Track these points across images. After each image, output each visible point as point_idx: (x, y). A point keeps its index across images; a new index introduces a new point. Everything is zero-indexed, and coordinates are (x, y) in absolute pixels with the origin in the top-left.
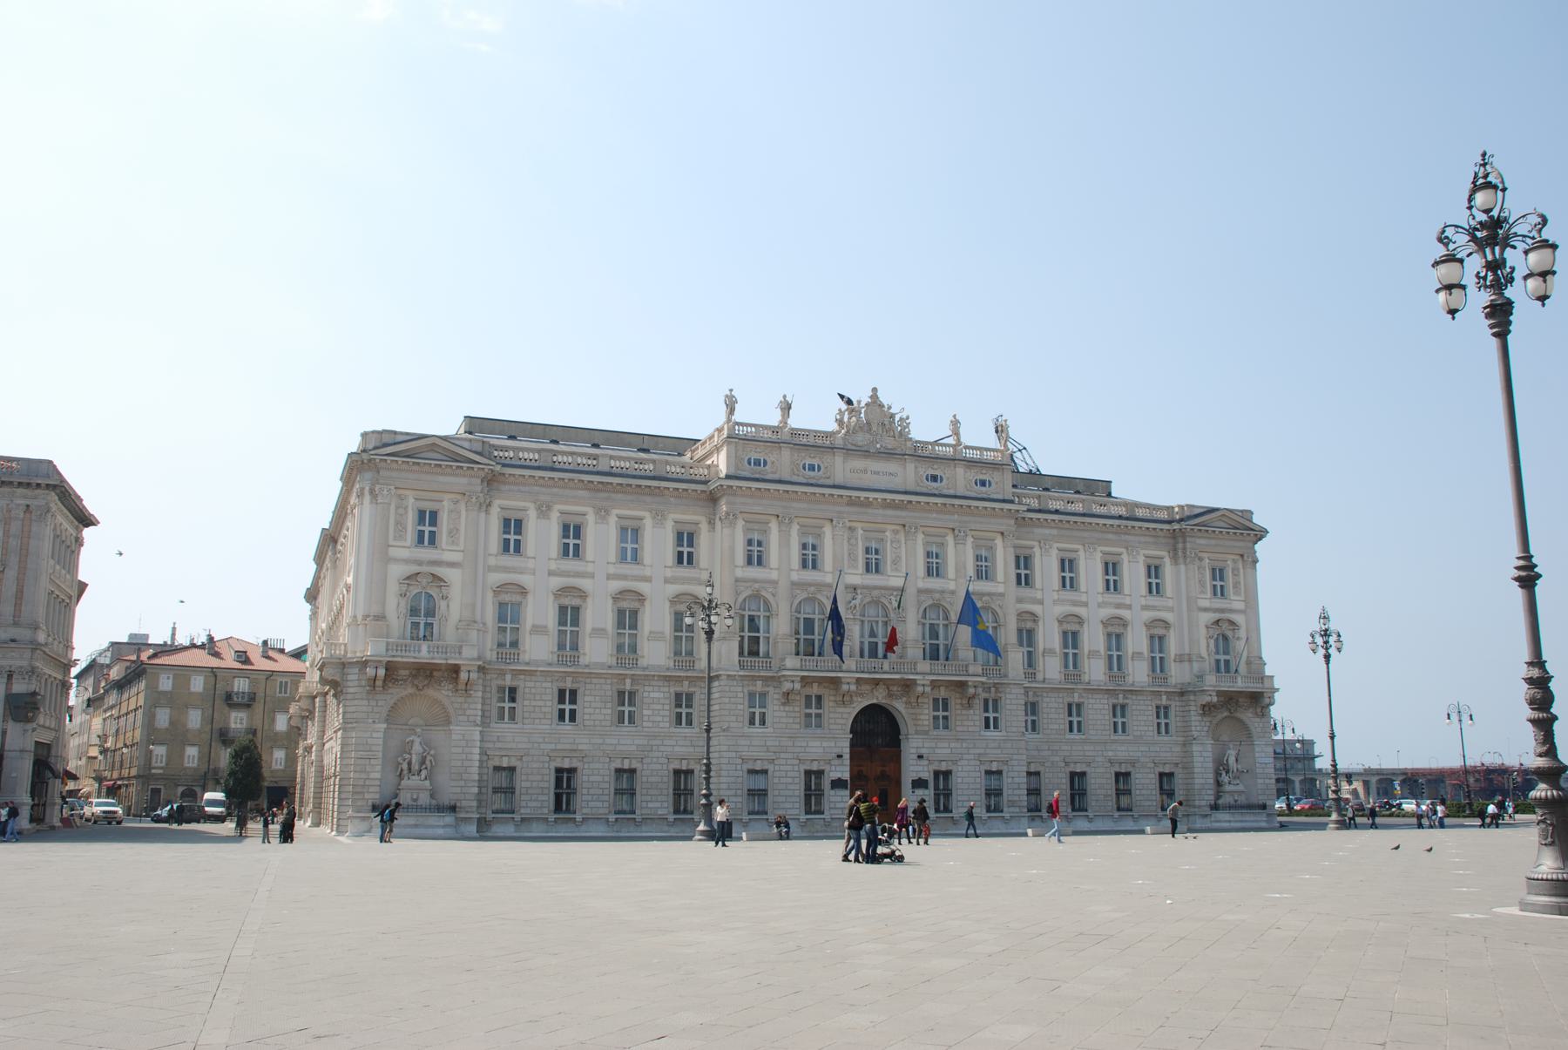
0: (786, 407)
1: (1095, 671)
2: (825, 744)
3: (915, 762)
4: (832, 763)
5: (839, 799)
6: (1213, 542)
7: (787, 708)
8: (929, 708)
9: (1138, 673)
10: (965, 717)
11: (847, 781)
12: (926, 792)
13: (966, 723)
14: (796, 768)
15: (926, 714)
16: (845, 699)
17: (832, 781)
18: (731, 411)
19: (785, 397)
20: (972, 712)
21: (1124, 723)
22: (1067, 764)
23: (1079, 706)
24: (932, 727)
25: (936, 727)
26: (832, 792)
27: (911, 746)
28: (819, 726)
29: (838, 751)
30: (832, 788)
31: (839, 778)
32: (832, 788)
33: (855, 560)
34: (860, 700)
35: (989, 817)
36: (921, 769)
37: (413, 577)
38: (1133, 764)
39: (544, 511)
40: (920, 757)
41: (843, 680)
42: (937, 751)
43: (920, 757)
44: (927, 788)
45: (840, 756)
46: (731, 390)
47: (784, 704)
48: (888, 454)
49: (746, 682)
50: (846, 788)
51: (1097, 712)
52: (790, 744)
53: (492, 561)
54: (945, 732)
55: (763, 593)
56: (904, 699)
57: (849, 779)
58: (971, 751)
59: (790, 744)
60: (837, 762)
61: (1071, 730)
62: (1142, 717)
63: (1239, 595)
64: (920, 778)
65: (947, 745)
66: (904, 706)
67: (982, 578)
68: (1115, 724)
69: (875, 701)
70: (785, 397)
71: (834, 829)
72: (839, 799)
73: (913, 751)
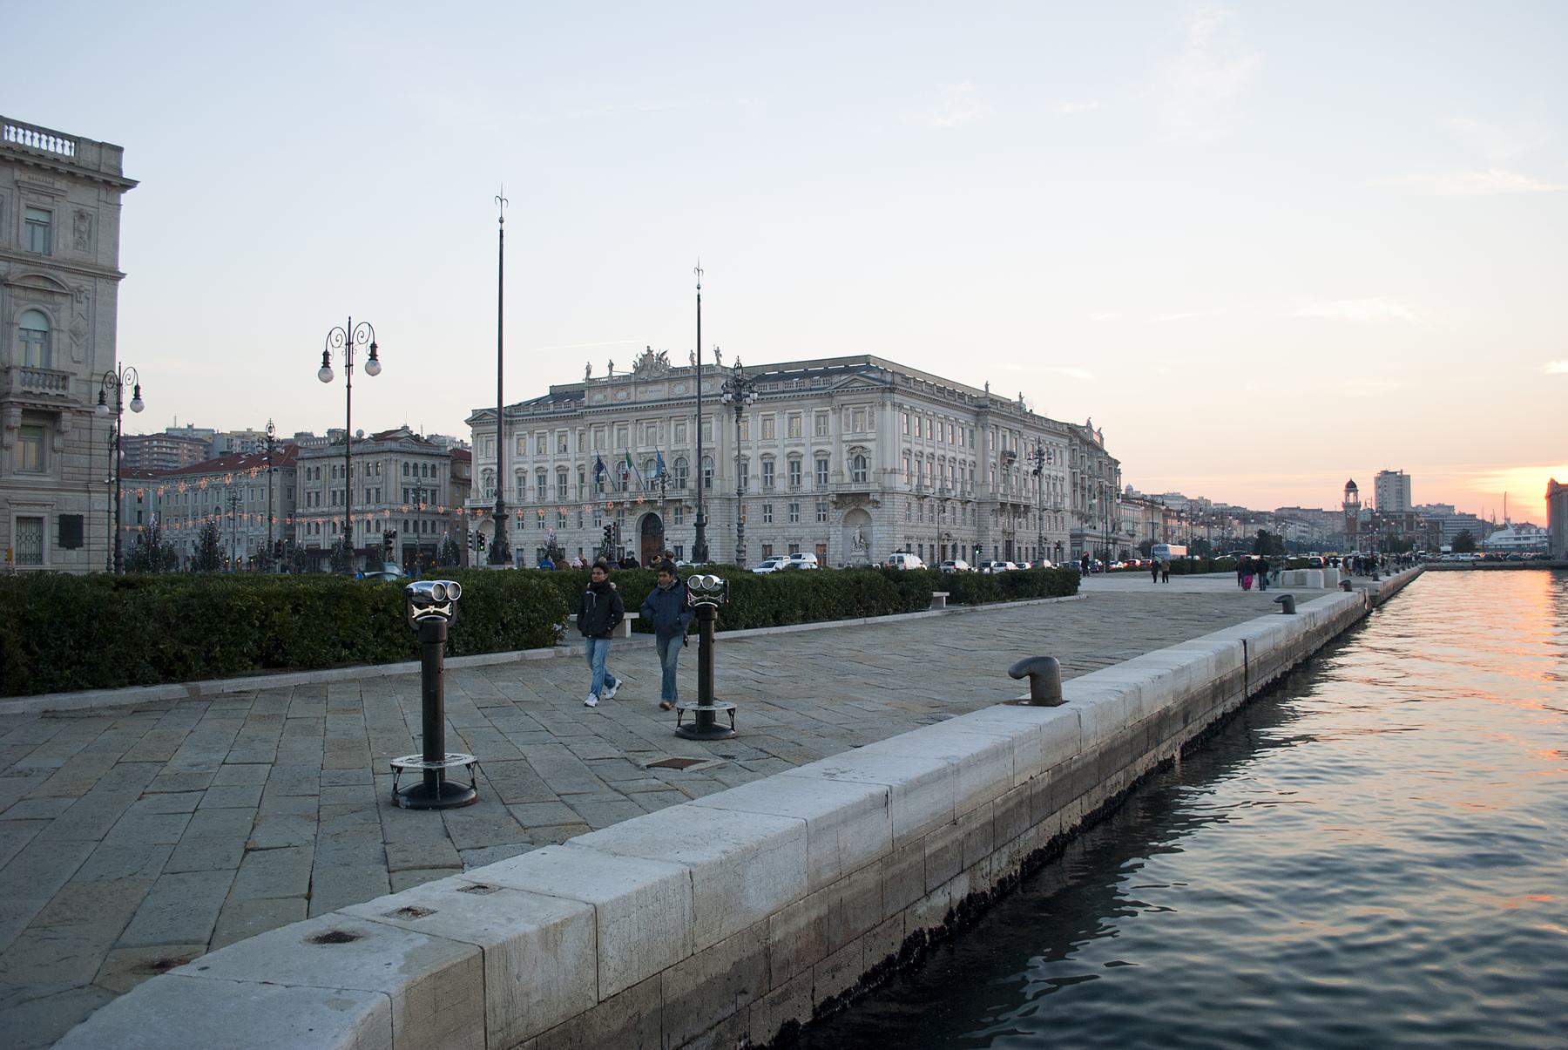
0: (611, 365)
1: (781, 486)
6: (852, 397)
9: (808, 485)
15: (671, 515)
16: (631, 511)
18: (589, 373)
21: (770, 516)
22: (761, 541)
23: (770, 506)
25: (676, 523)
27: (667, 534)
33: (642, 439)
37: (485, 470)
38: (800, 539)
39: (531, 433)
40: (667, 539)
43: (667, 539)
48: (656, 381)
51: (780, 508)
53: (515, 460)
60: (629, 543)
61: (766, 521)
62: (808, 511)
63: (873, 428)
68: (765, 517)
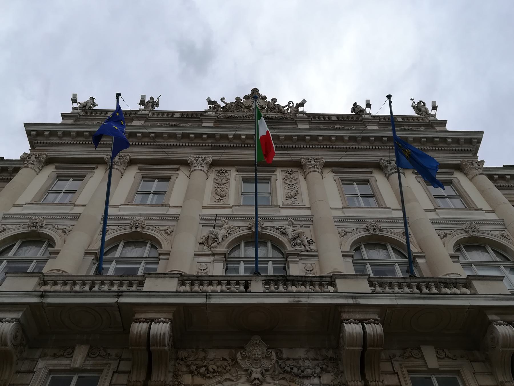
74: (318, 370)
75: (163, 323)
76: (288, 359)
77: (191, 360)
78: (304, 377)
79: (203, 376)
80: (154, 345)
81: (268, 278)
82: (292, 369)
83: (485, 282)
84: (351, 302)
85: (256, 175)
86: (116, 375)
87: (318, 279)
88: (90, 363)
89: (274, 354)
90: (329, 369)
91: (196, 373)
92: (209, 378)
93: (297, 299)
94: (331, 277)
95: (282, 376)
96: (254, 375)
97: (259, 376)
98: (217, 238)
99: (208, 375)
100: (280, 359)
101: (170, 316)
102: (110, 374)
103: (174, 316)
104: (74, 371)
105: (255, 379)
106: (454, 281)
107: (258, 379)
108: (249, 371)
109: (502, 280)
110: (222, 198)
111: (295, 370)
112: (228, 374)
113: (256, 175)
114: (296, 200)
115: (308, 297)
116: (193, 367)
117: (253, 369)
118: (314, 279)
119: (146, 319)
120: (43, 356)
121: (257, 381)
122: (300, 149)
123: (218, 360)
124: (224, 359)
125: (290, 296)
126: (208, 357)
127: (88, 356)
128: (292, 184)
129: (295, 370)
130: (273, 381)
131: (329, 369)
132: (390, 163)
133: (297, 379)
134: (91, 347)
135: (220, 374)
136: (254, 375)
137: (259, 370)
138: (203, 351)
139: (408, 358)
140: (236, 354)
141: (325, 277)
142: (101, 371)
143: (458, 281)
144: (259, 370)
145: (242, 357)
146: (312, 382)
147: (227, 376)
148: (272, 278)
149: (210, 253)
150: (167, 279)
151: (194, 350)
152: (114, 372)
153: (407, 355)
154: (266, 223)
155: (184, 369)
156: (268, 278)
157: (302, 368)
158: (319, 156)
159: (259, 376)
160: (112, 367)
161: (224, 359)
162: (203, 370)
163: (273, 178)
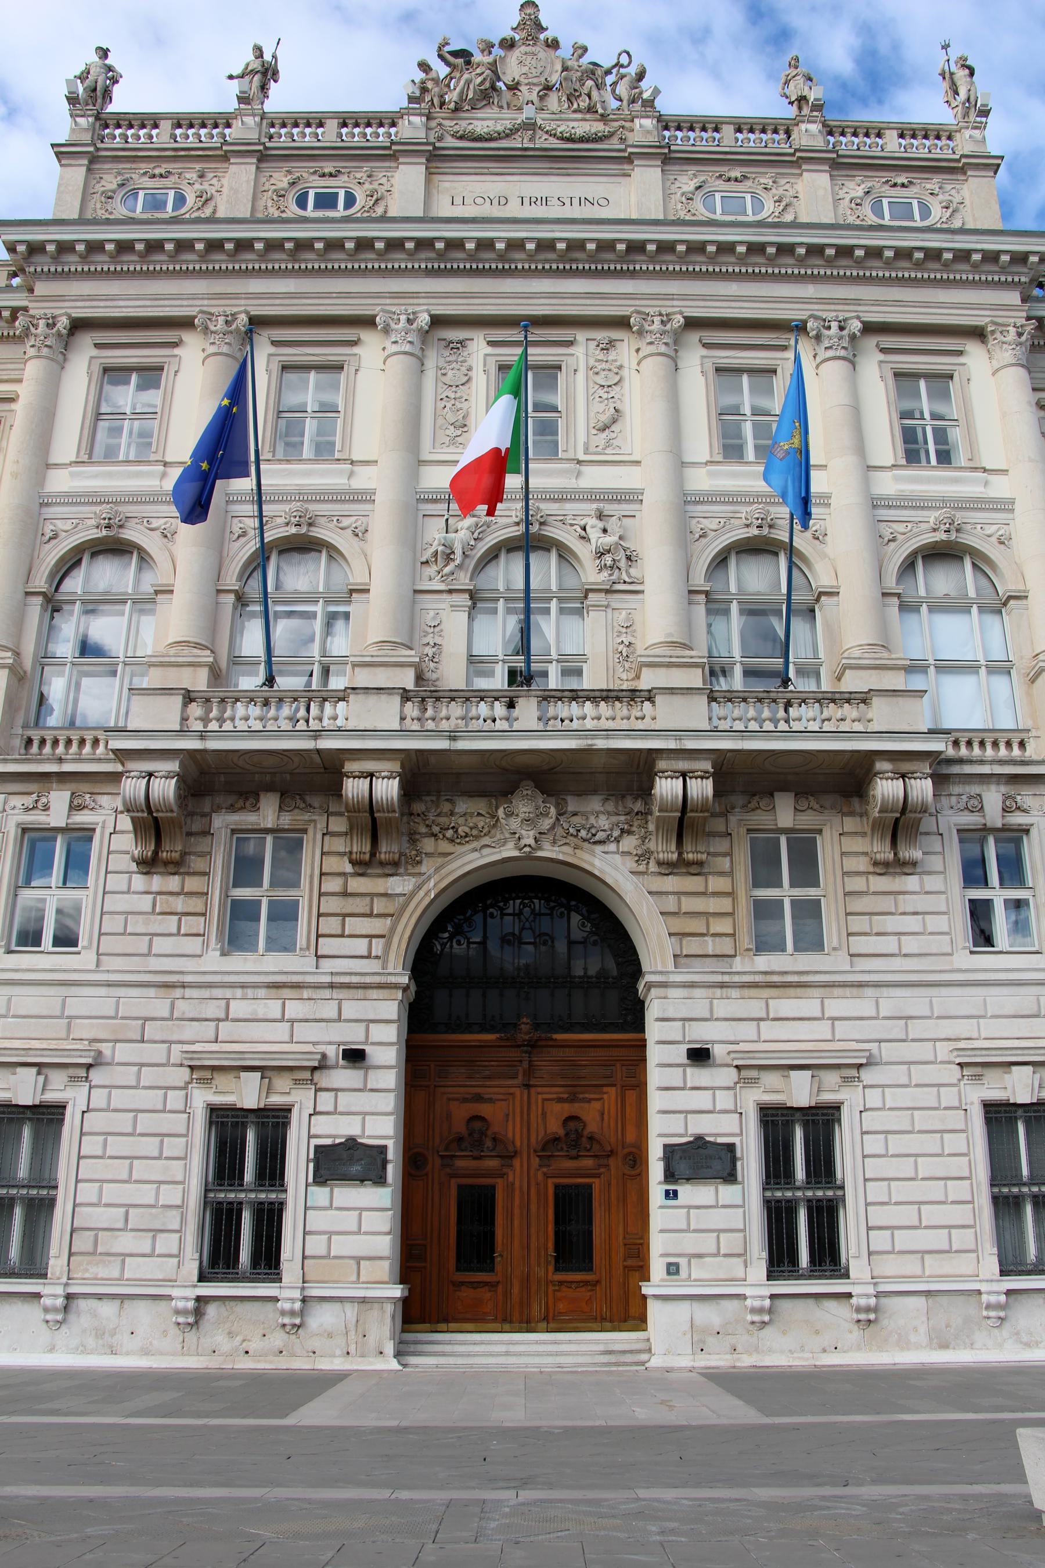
2: (294, 1009)
3: (674, 1077)
4: (324, 1079)
5: (349, 1220)
7: (157, 882)
8: (730, 874)
10: (886, 903)
11: (383, 1149)
12: (728, 1193)
13: (891, 923)
14: (175, 1099)
17: (317, 1148)
19: (259, 51)
20: (912, 882)
24: (746, 940)
25: (765, 944)
26: (320, 1195)
28: (280, 944)
29: (353, 1036)
30: (322, 1176)
31: (351, 1144)
32: (322, 1176)
34: (444, 846)
35: (1009, 1293)
36: (702, 1101)
40: (699, 1056)
41: (350, 767)
42: (769, 1030)
43: (699, 1056)
44: (730, 1177)
45: (355, 1056)
46: (104, 53)
47: (148, 865)
49: (17, 801)
50: (380, 1180)
52: (162, 1008)
54: (807, 961)
55: (130, 534)
56: (629, 843)
57: (390, 1144)
58: (916, 1029)
59: (162, 1008)
60: (344, 1077)
64: (699, 1139)
65: (808, 1005)
66: (630, 863)
67: (929, 462)
69: (509, 851)
70: (259, 51)
71: (315, 1343)
72: (349, 1220)
73: (673, 1030)
74: (616, 833)
75: (389, 778)
76: (575, 814)
77: (431, 817)
78: (595, 843)
79: (451, 841)
80: (379, 811)
81: (547, 693)
82: (579, 831)
83: (895, 699)
84: (672, 745)
85: (526, 337)
86: (327, 838)
87: (628, 693)
88: (286, 820)
89: (553, 811)
90: (634, 829)
91: (441, 836)
92: (459, 844)
93: (590, 742)
94: (649, 691)
95: (565, 841)
96: (523, 842)
97: (531, 842)
98: (453, 552)
99: (458, 841)
100: (560, 815)
101: (396, 766)
102: (319, 836)
103: (402, 766)
104: (267, 831)
105: (525, 846)
106: (847, 696)
107: (530, 846)
108: (517, 836)
109: (922, 697)
110: (459, 432)
111: (583, 833)
112: (487, 838)
113: (526, 337)
114: (613, 435)
115: (607, 737)
116: (436, 829)
117: (523, 832)
118: (620, 694)
119: (363, 772)
120: (217, 809)
121: (527, 849)
122: (633, 274)
123: (471, 815)
124: (479, 814)
125: (580, 738)
126: (456, 810)
127: (281, 809)
128: (609, 386)
129: (583, 833)
130: (551, 848)
131: (634, 829)
132: (829, 328)
133: (586, 844)
134: (282, 795)
135: (477, 838)
136: (523, 842)
137: (532, 833)
138: (447, 800)
139: (753, 810)
140: (497, 808)
141: (641, 691)
142: (305, 831)
143: (853, 696)
144: (532, 833)
145: (505, 814)
146: (606, 850)
147: (486, 841)
148: (553, 693)
149: (442, 587)
150: (384, 697)
151: (434, 798)
152: (324, 834)
153: (752, 805)
154: (547, 508)
155: (423, 829)
156: (547, 693)
157: (593, 831)
158: (673, 299)
159: (531, 842)
160: (319, 826)
161: (479, 814)
162: (450, 833)
163: (568, 363)
